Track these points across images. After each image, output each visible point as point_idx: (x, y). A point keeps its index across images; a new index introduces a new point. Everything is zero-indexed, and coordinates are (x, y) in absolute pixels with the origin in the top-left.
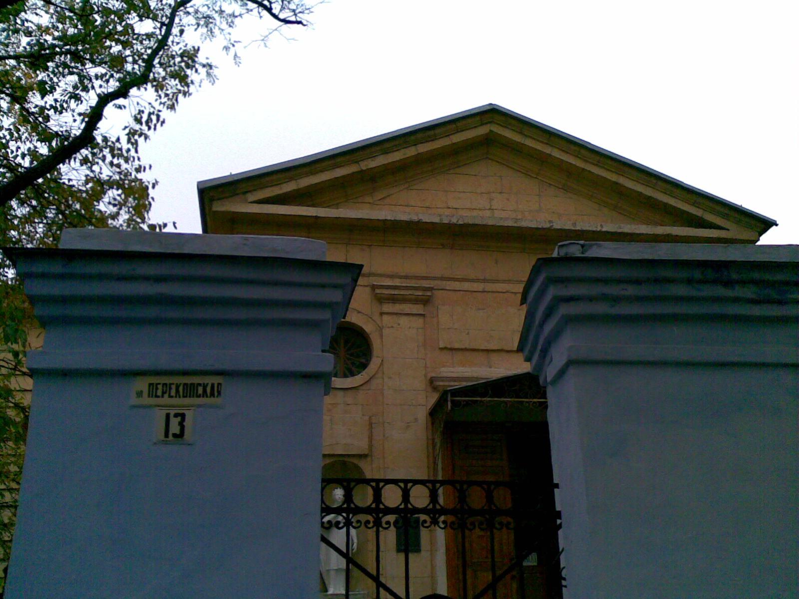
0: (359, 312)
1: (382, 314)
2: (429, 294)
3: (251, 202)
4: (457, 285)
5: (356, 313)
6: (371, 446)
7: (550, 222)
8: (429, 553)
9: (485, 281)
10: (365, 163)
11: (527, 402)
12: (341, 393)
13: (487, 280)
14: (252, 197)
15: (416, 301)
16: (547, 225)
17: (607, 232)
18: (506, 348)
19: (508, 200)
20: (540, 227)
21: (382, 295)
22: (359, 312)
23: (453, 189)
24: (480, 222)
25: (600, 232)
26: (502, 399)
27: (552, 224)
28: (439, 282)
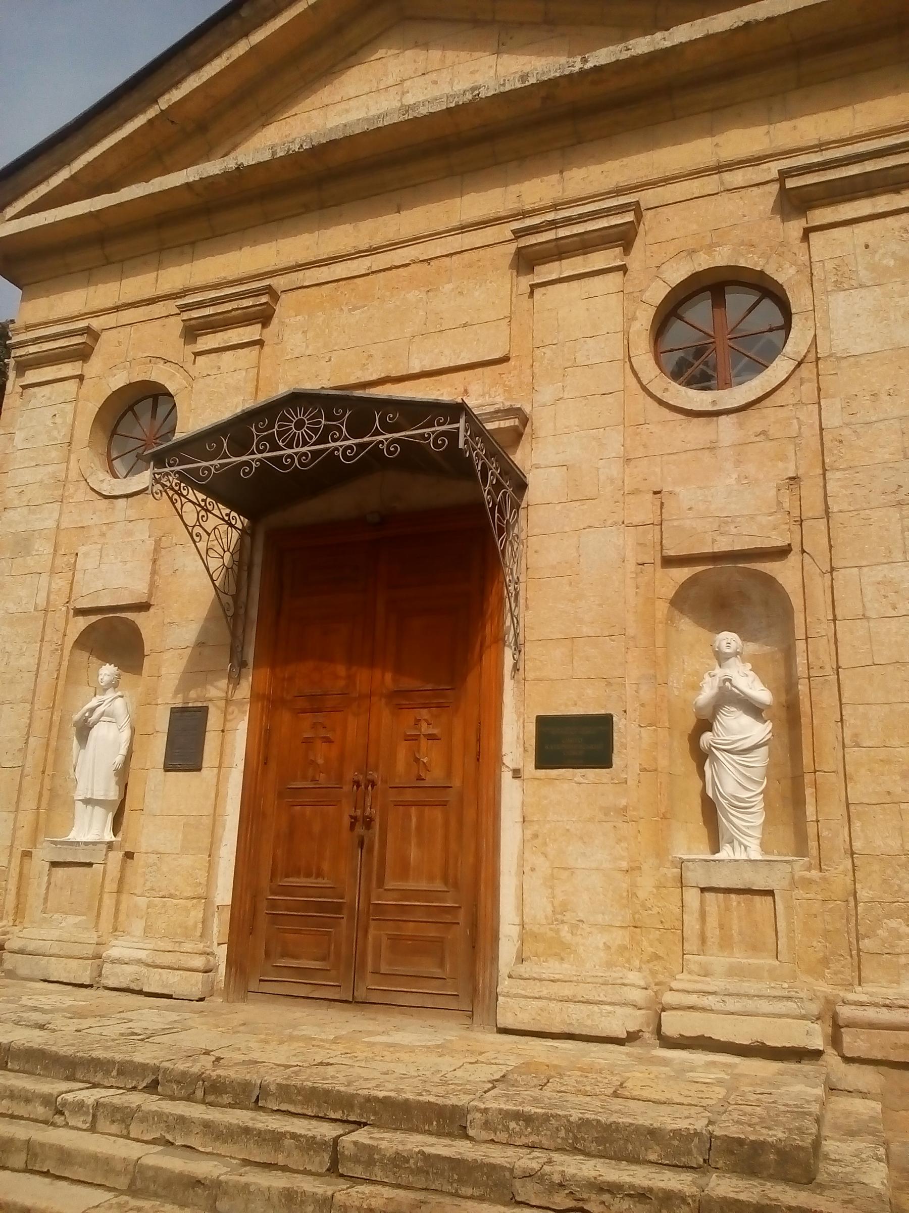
0: (166, 361)
1: (197, 354)
2: (264, 299)
3: (9, 220)
4: (324, 274)
5: (161, 365)
6: (152, 585)
7: (473, 89)
8: (216, 771)
9: (372, 251)
10: (167, 97)
11: (290, 456)
12: (122, 502)
13: (375, 249)
14: (10, 211)
15: (246, 319)
16: (469, 96)
17: (597, 69)
18: (394, 374)
19: (435, 82)
20: (453, 105)
21: (193, 322)
22: (166, 362)
23: (338, 98)
24: (340, 134)
25: (583, 73)
26: (244, 458)
27: (477, 92)
28: (294, 276)
